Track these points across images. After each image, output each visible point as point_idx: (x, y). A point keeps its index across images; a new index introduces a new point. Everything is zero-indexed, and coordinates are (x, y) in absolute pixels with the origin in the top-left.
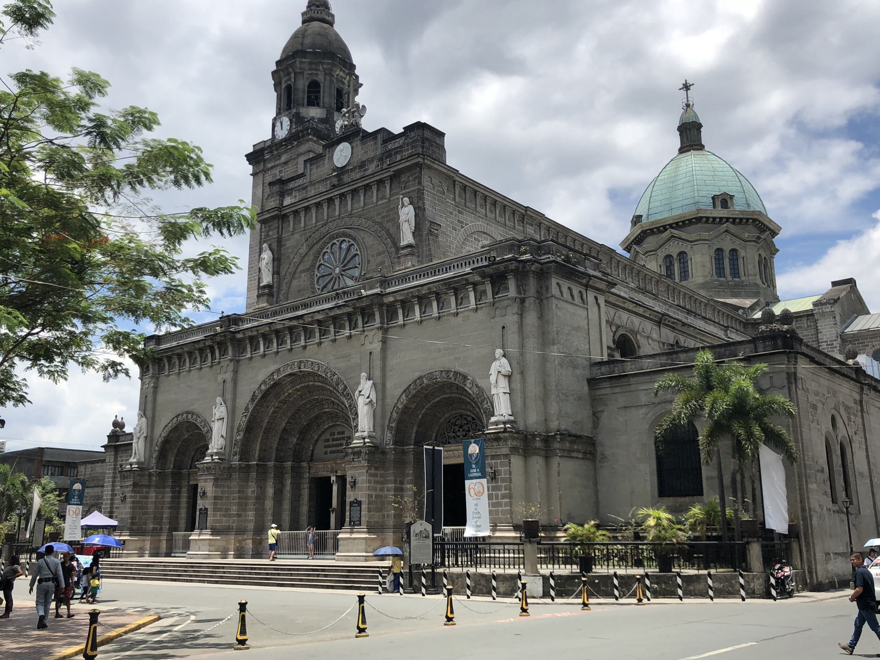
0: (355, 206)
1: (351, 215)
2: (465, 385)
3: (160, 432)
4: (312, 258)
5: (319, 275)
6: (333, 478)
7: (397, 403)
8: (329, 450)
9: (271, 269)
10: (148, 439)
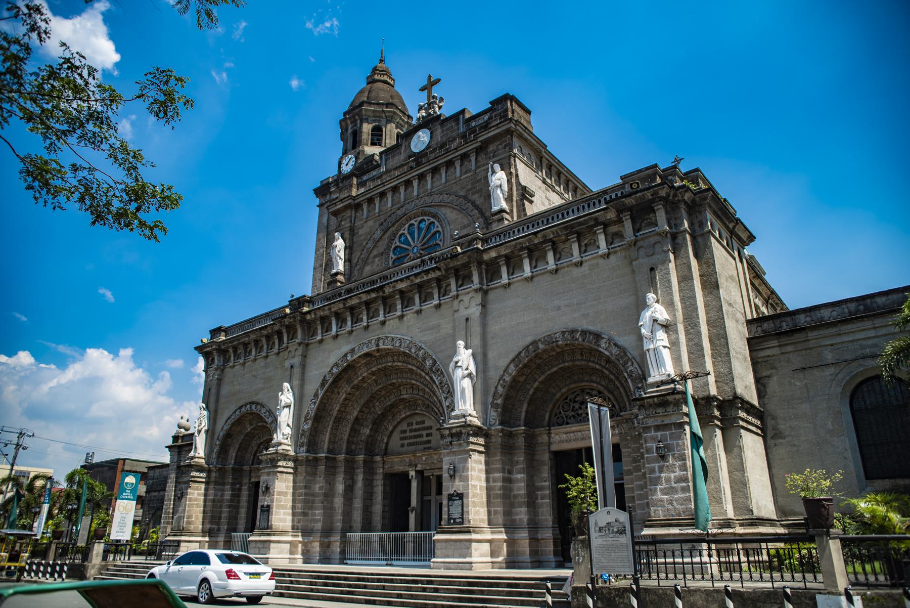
0: (437, 184)
1: (431, 194)
2: (599, 346)
3: (222, 426)
4: (387, 241)
5: (394, 257)
6: (412, 473)
7: (503, 375)
8: (406, 442)
9: (343, 257)
10: (210, 433)
